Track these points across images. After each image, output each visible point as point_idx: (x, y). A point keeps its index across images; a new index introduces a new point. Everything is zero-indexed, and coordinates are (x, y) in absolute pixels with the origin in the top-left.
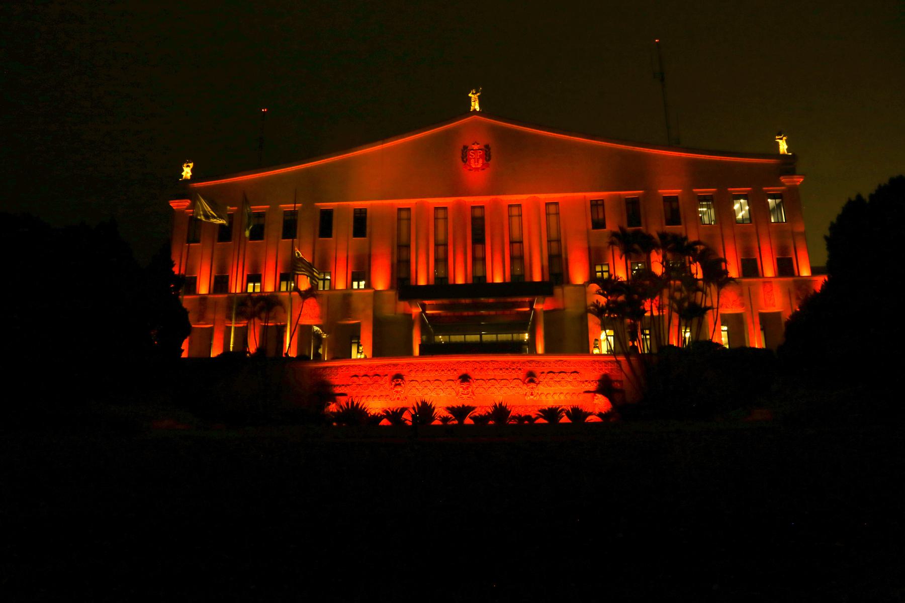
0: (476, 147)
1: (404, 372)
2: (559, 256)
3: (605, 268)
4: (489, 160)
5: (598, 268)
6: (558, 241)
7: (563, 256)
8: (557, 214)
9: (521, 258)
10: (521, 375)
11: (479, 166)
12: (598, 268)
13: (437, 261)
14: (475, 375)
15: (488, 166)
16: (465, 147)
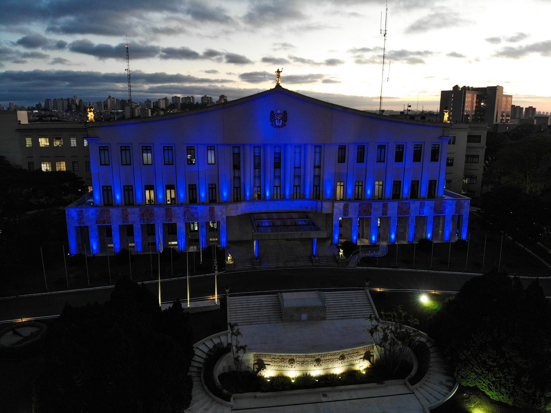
0: (279, 112)
1: (294, 358)
2: (319, 176)
3: (342, 184)
4: (286, 121)
5: (338, 184)
6: (319, 167)
7: (321, 177)
8: (320, 153)
9: (299, 177)
10: (338, 357)
11: (280, 125)
12: (338, 184)
13: (255, 177)
14: (322, 359)
15: (285, 125)
16: (272, 112)
